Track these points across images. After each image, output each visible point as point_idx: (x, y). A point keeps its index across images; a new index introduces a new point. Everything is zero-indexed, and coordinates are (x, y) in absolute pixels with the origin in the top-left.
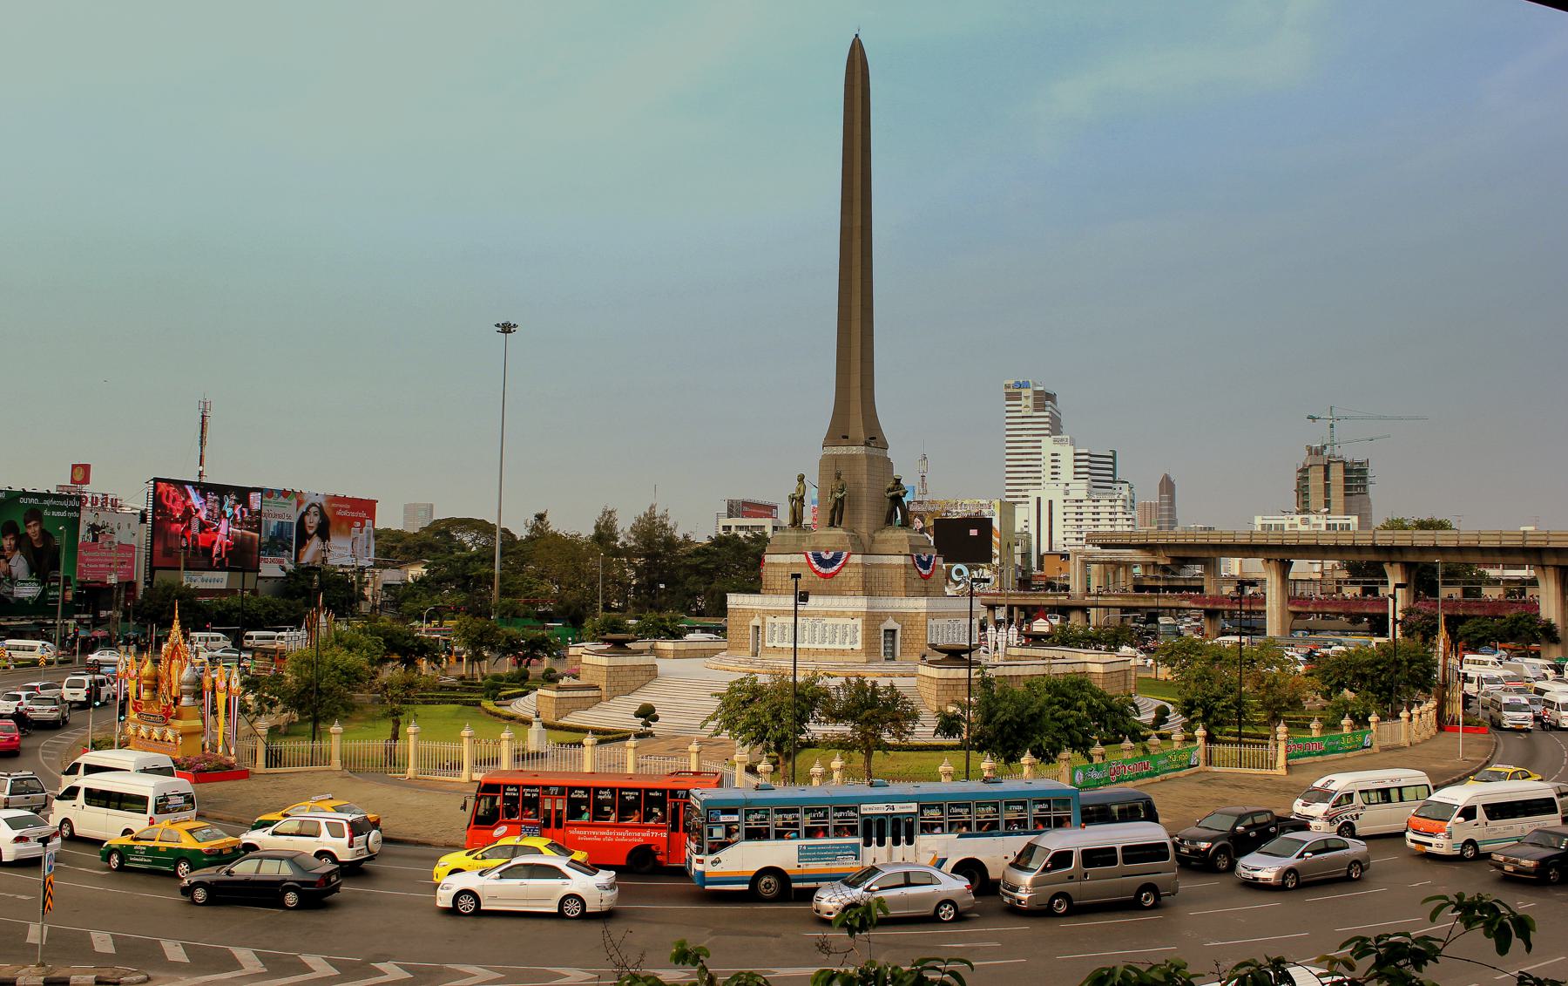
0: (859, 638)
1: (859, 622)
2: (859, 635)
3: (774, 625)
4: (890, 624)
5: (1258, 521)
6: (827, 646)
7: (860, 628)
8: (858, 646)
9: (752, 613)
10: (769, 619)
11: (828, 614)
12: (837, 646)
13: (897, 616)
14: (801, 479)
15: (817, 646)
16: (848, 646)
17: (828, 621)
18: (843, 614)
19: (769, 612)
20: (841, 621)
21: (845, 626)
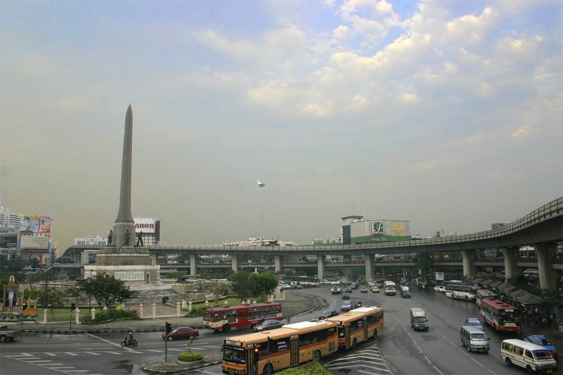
1: (143, 272)
2: (143, 276)
4: (148, 273)
5: (77, 240)
6: (134, 279)
7: (143, 274)
8: (143, 279)
10: (116, 273)
11: (134, 270)
12: (137, 279)
13: (150, 270)
14: (111, 231)
15: (130, 280)
16: (140, 279)
17: (134, 272)
18: (138, 270)
19: (116, 271)
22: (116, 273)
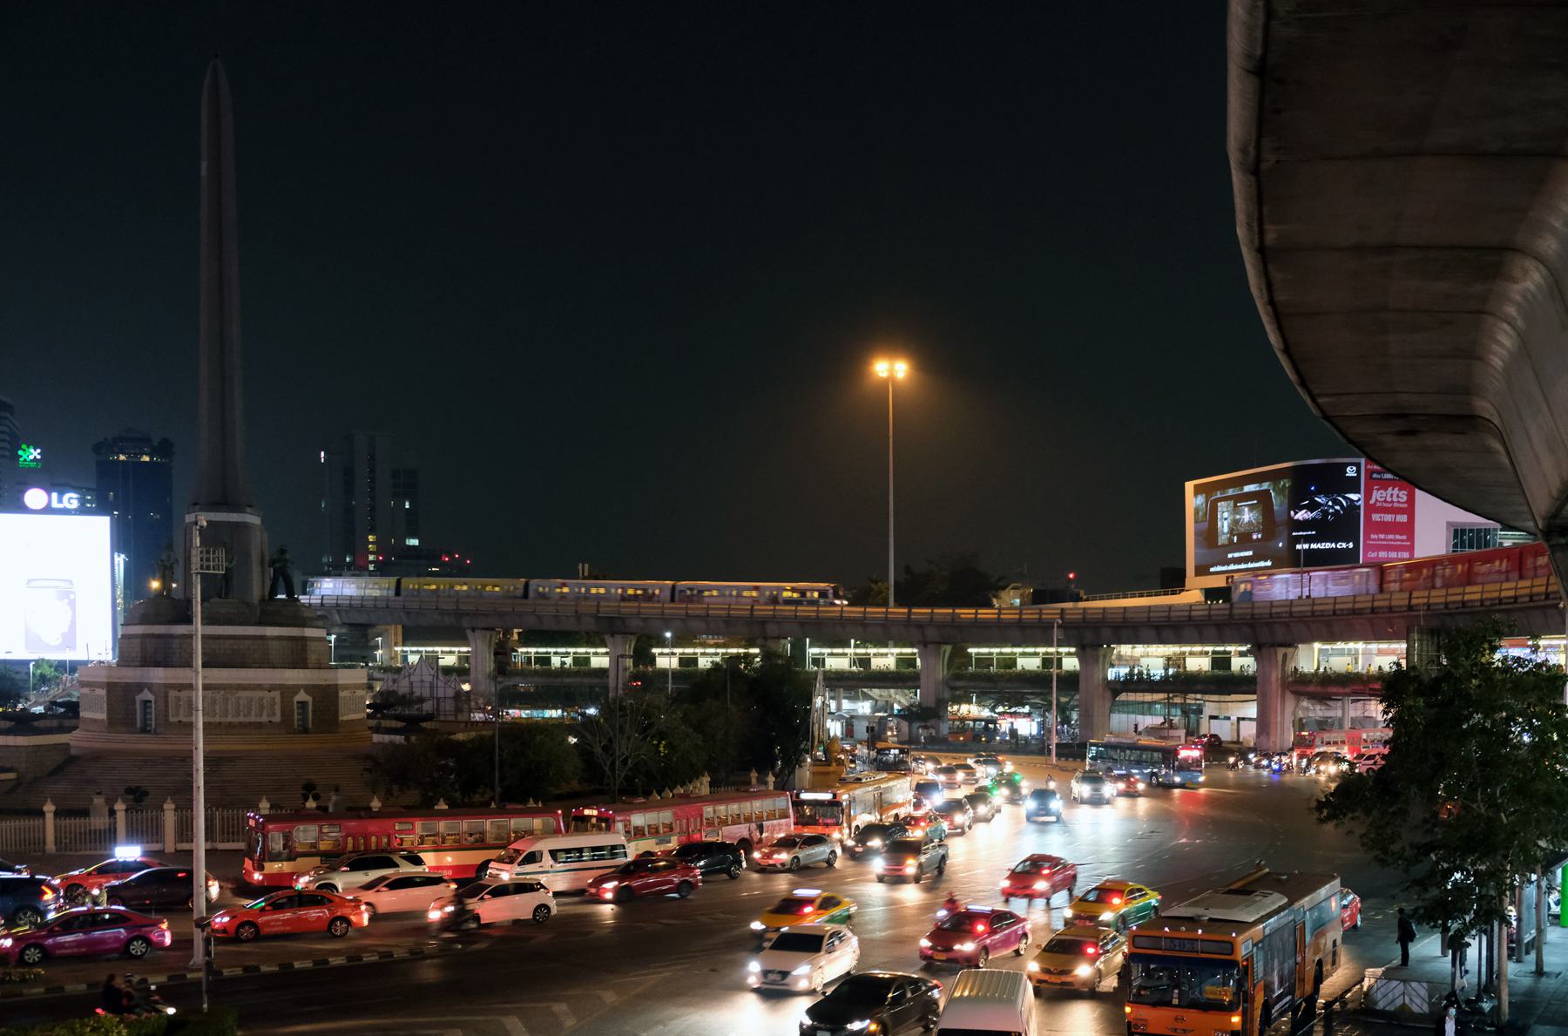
0: (278, 712)
1: (276, 694)
3: (178, 699)
4: (302, 696)
6: (241, 719)
7: (278, 700)
8: (277, 718)
9: (140, 687)
10: (172, 694)
12: (252, 719)
13: (309, 689)
15: (229, 719)
16: (264, 719)
17: (242, 694)
18: (259, 687)
20: (258, 694)
21: (261, 699)
22: (172, 694)
